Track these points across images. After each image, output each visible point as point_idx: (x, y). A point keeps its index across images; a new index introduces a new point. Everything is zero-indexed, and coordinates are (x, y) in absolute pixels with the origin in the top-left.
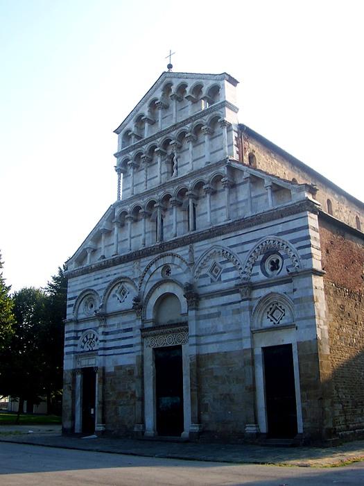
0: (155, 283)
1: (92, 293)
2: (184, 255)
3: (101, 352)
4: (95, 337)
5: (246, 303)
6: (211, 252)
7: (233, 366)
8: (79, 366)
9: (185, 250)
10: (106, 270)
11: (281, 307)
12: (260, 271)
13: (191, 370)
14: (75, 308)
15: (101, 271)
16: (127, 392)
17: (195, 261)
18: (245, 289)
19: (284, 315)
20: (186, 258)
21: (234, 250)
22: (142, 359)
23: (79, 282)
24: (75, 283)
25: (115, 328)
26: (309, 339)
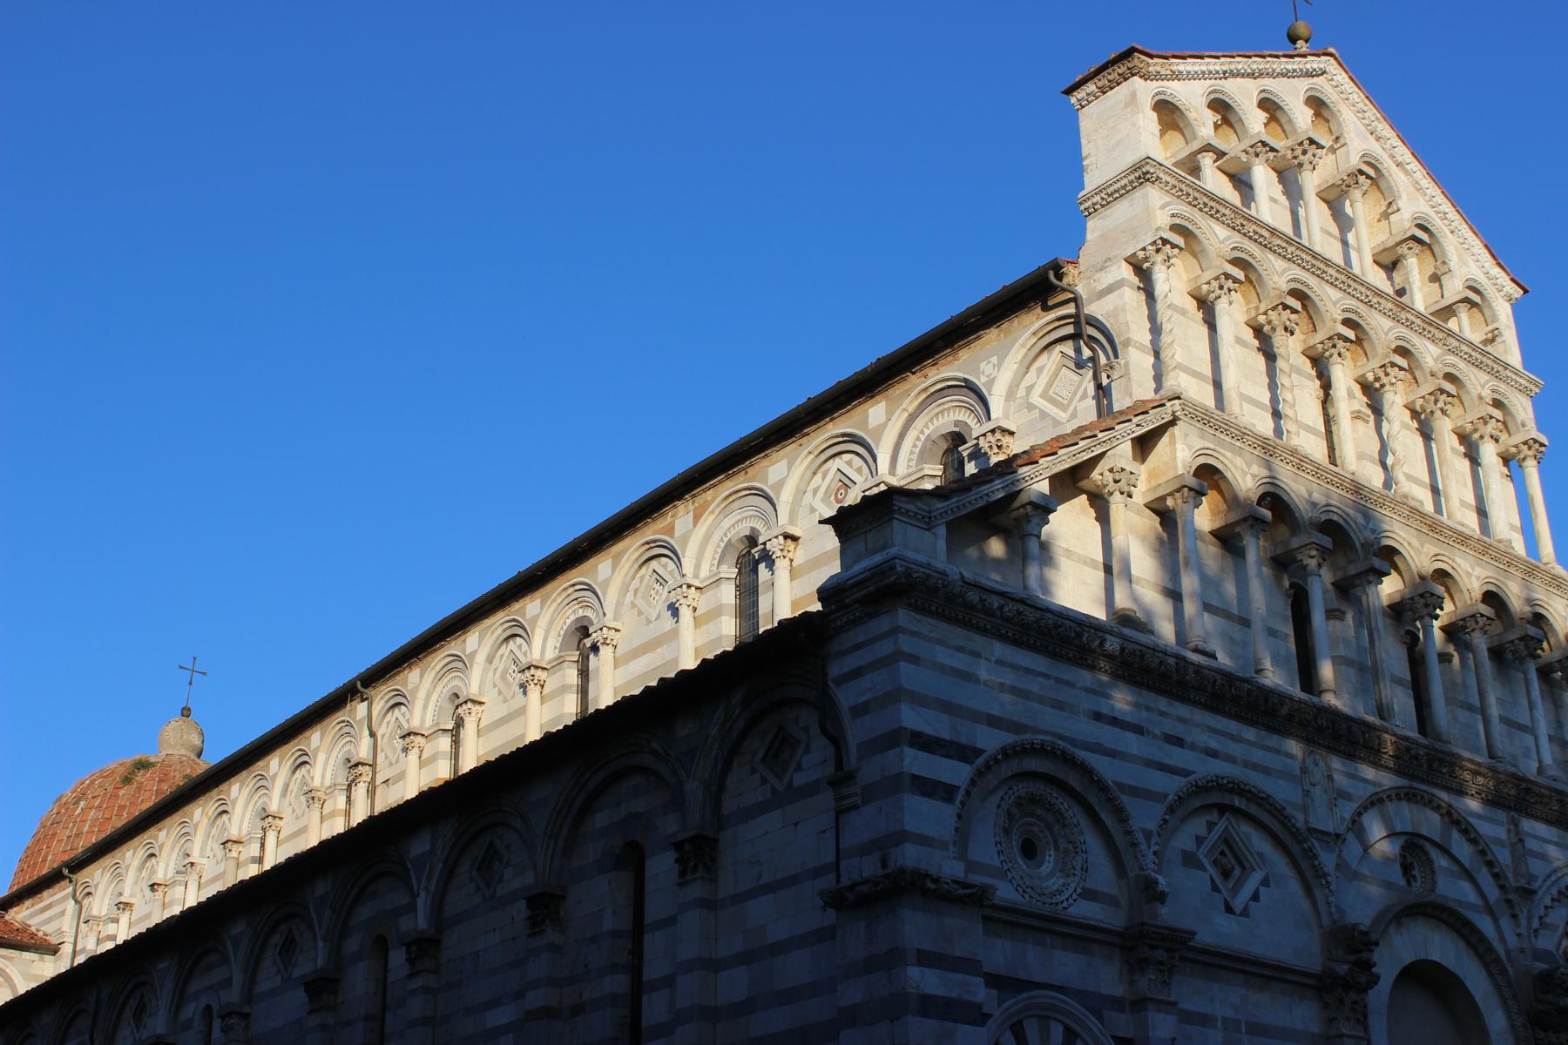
1: (1073, 780)
10: (1162, 703)
17: (1535, 885)
24: (959, 661)
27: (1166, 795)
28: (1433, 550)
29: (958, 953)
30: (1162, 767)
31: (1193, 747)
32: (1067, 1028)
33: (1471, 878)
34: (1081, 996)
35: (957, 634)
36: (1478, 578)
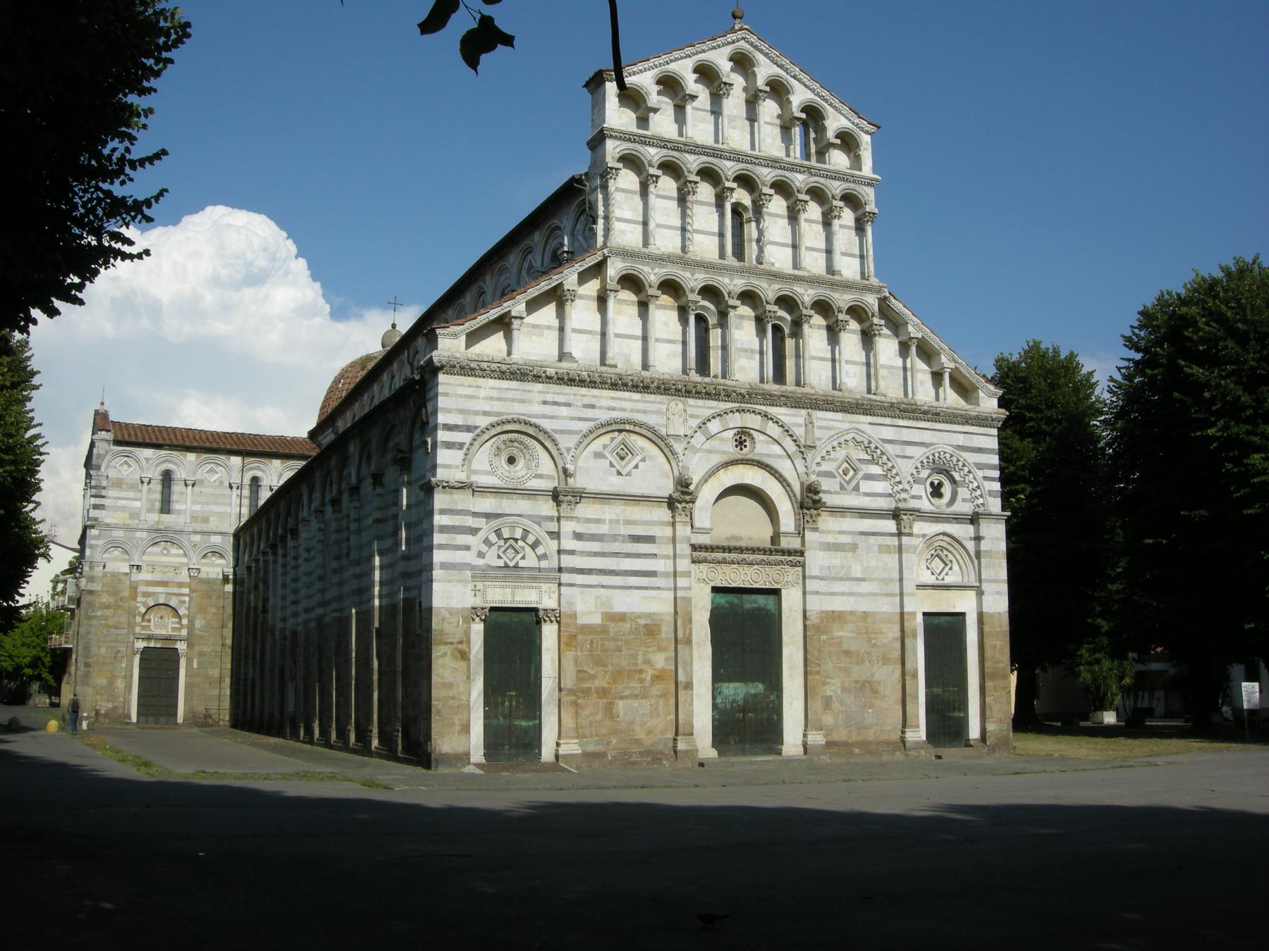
0: (717, 459)
1: (531, 431)
3: (565, 577)
4: (531, 539)
6: (847, 437)
7: (878, 636)
8: (478, 602)
9: (796, 416)
10: (584, 391)
11: (946, 556)
16: (641, 672)
17: (818, 444)
18: (911, 517)
19: (951, 569)
22: (681, 611)
23: (482, 393)
25: (603, 529)
26: (999, 611)
27: (581, 431)
28: (777, 287)
29: (459, 508)
30: (580, 419)
31: (600, 408)
33: (780, 444)
34: (529, 517)
35: (470, 380)
36: (808, 295)
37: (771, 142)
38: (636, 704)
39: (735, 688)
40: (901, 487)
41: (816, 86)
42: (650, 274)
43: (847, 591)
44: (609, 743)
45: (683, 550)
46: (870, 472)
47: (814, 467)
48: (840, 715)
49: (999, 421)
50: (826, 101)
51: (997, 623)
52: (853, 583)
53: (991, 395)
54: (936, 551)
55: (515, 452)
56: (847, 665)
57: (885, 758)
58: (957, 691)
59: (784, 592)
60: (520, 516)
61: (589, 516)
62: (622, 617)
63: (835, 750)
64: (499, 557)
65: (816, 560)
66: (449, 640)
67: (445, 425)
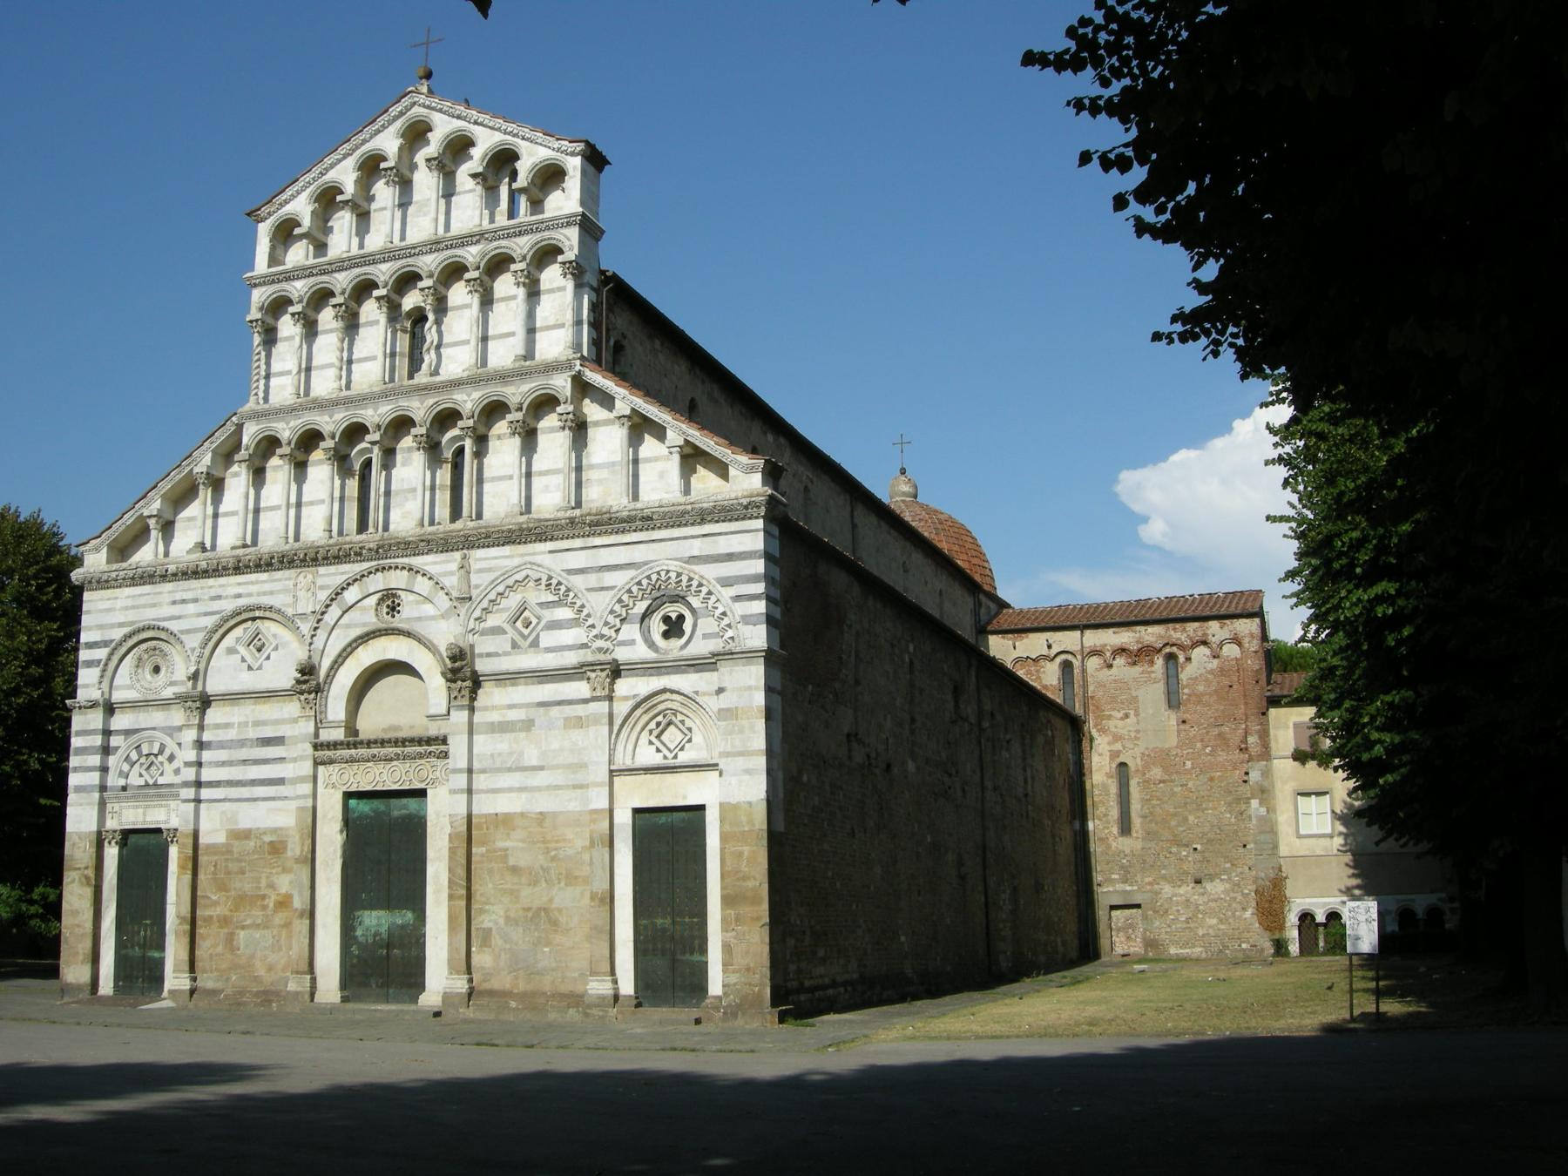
1: (163, 635)
2: (446, 574)
4: (167, 753)
5: (603, 707)
7: (558, 845)
8: (111, 824)
9: (448, 562)
10: (211, 581)
11: (682, 722)
12: (638, 637)
13: (452, 851)
14: (104, 671)
15: (194, 583)
16: (264, 897)
17: (474, 593)
20: (451, 582)
21: (578, 582)
23: (119, 604)
24: (107, 605)
25: (232, 734)
29: (92, 728)
30: (206, 614)
31: (227, 597)
32: (161, 744)
35: (109, 592)
37: (469, 210)
38: (257, 934)
39: (379, 918)
40: (595, 632)
41: (499, 122)
42: (284, 429)
43: (518, 786)
44: (228, 980)
45: (304, 750)
46: (555, 618)
47: (471, 624)
48: (503, 956)
49: (758, 507)
50: (516, 135)
51: (744, 819)
52: (526, 773)
53: (750, 470)
54: (664, 717)
55: (159, 661)
56: (516, 887)
57: (552, 1016)
58: (697, 924)
59: (428, 791)
60: (154, 729)
61: (218, 721)
62: (246, 835)
63: (483, 1001)
64: (141, 775)
65: (457, 746)
66: (78, 866)
67: (86, 644)
